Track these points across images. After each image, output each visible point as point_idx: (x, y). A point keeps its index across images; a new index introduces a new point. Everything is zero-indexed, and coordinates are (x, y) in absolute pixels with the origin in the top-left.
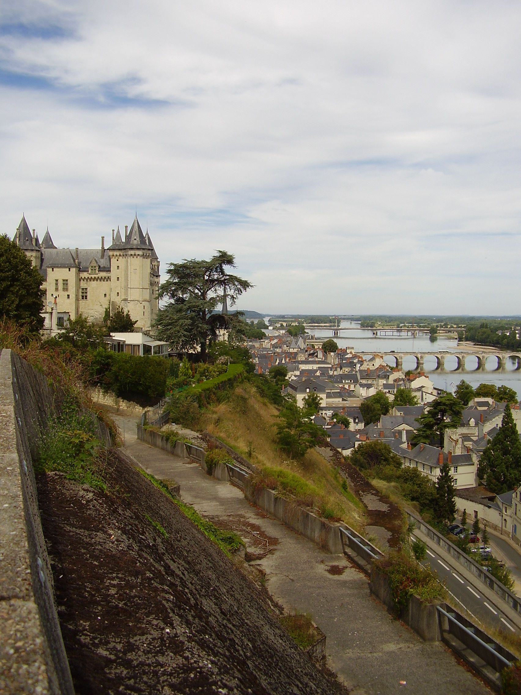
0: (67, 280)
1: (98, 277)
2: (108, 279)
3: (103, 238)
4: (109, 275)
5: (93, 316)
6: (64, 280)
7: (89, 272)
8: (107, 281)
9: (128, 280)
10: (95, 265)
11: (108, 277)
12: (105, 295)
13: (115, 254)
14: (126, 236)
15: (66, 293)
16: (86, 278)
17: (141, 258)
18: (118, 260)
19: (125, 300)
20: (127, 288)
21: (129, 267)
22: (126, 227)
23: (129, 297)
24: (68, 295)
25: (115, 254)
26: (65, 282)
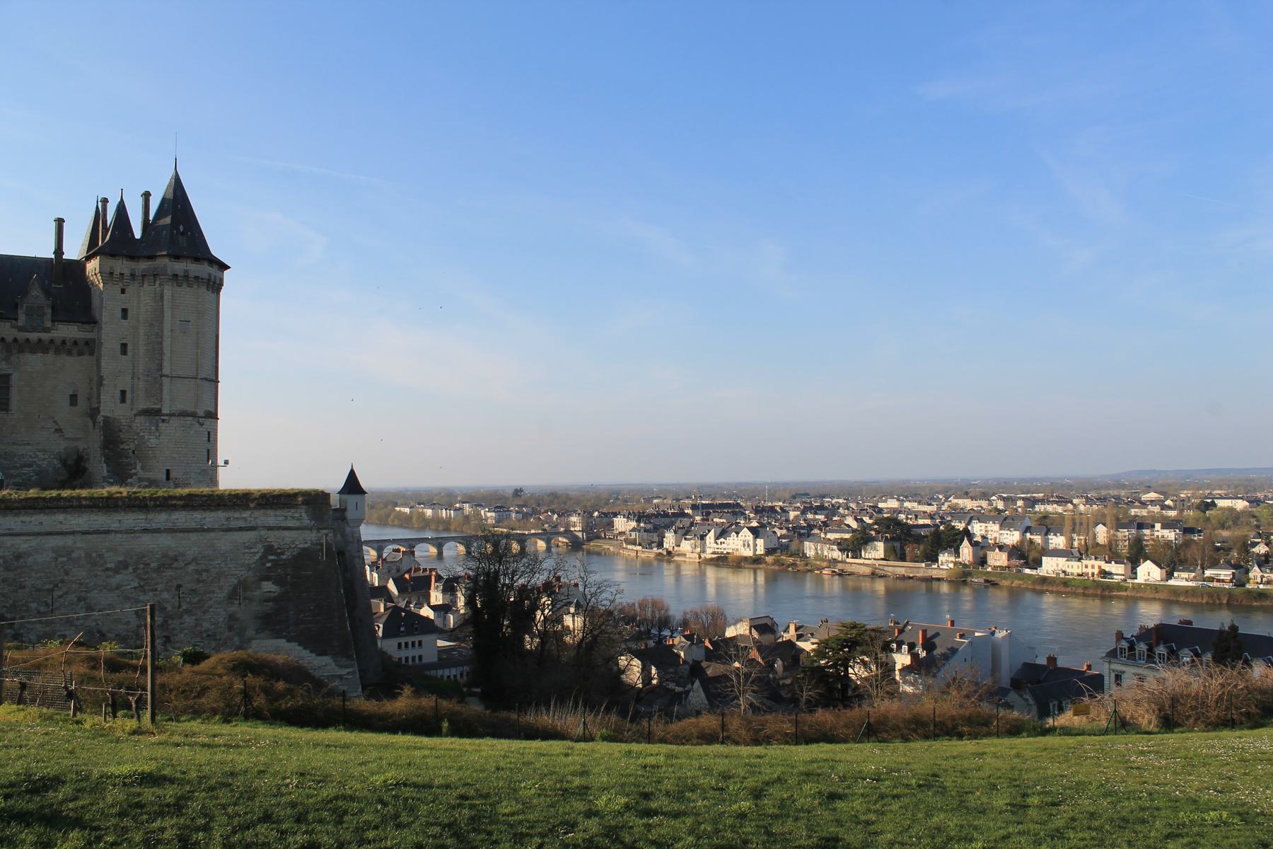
1: (52, 341)
3: (60, 223)
4: (88, 336)
5: (30, 466)
7: (20, 323)
8: (81, 354)
9: (162, 354)
13: (117, 272)
14: (146, 224)
17: (203, 290)
18: (123, 291)
19: (153, 413)
20: (157, 375)
21: (168, 313)
22: (147, 196)
25: (117, 272)
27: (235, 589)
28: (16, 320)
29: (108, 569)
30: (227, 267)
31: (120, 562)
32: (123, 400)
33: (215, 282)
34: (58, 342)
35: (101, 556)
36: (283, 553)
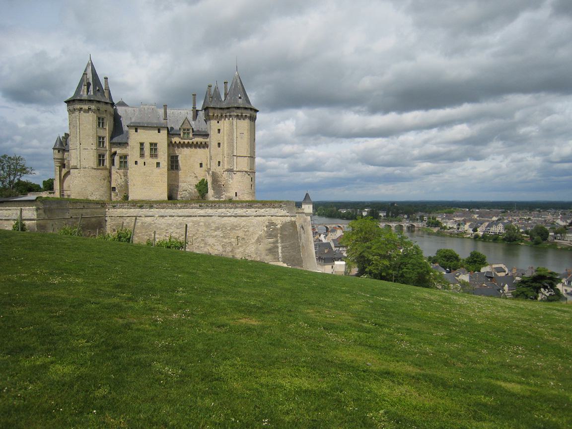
0: (156, 144)
1: (193, 142)
2: (205, 146)
4: (206, 140)
5: (186, 191)
6: (151, 144)
7: (182, 135)
9: (233, 146)
10: (189, 127)
11: (205, 143)
12: (201, 165)
15: (155, 161)
16: (178, 142)
18: (218, 122)
19: (230, 171)
21: (235, 130)
23: (235, 166)
24: (158, 164)
26: (154, 146)
27: (258, 239)
28: (180, 134)
29: (212, 230)
30: (258, 111)
31: (216, 227)
32: (219, 165)
33: (253, 117)
34: (195, 143)
35: (209, 224)
36: (277, 225)
